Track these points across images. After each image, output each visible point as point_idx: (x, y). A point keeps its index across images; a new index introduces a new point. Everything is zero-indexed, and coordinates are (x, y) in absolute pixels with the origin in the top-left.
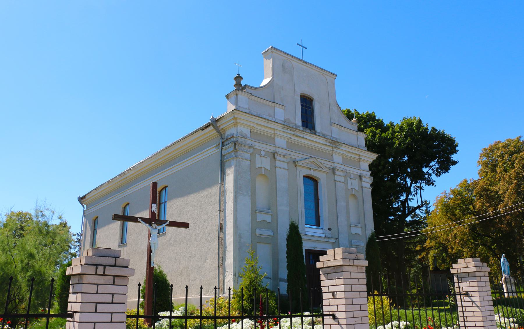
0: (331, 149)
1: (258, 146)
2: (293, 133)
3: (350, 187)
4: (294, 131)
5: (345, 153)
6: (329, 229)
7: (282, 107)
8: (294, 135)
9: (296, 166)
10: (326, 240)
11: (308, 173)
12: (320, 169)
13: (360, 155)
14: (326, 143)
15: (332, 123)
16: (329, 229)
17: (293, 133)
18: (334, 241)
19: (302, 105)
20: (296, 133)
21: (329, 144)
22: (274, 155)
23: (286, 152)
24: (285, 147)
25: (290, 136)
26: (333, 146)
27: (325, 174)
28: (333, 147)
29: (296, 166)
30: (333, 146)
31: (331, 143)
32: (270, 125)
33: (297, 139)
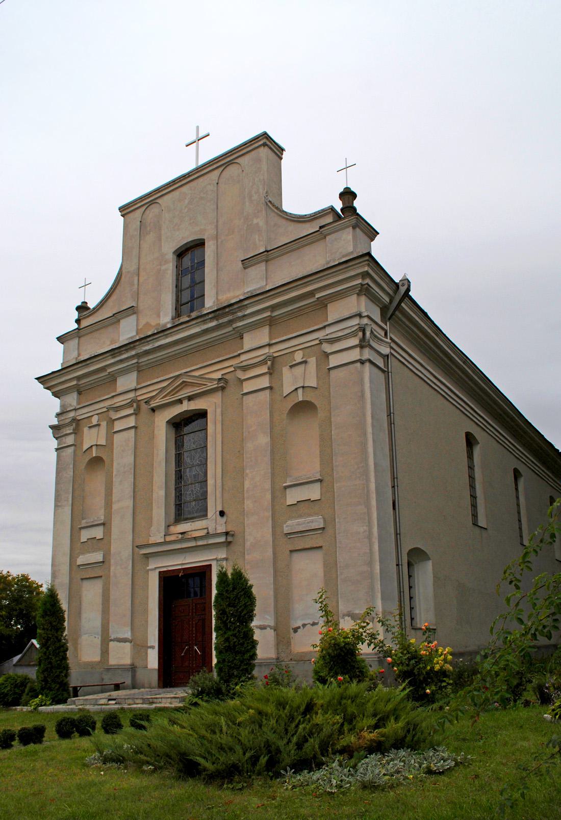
0: (231, 329)
1: (82, 414)
2: (133, 353)
3: (287, 390)
4: (133, 348)
6: (222, 514)
7: (130, 311)
9: (153, 410)
10: (211, 541)
13: (311, 294)
15: (247, 263)
16: (222, 514)
17: (133, 353)
18: (222, 539)
21: (214, 323)
25: (135, 361)
26: (225, 320)
30: (225, 320)
31: (216, 318)
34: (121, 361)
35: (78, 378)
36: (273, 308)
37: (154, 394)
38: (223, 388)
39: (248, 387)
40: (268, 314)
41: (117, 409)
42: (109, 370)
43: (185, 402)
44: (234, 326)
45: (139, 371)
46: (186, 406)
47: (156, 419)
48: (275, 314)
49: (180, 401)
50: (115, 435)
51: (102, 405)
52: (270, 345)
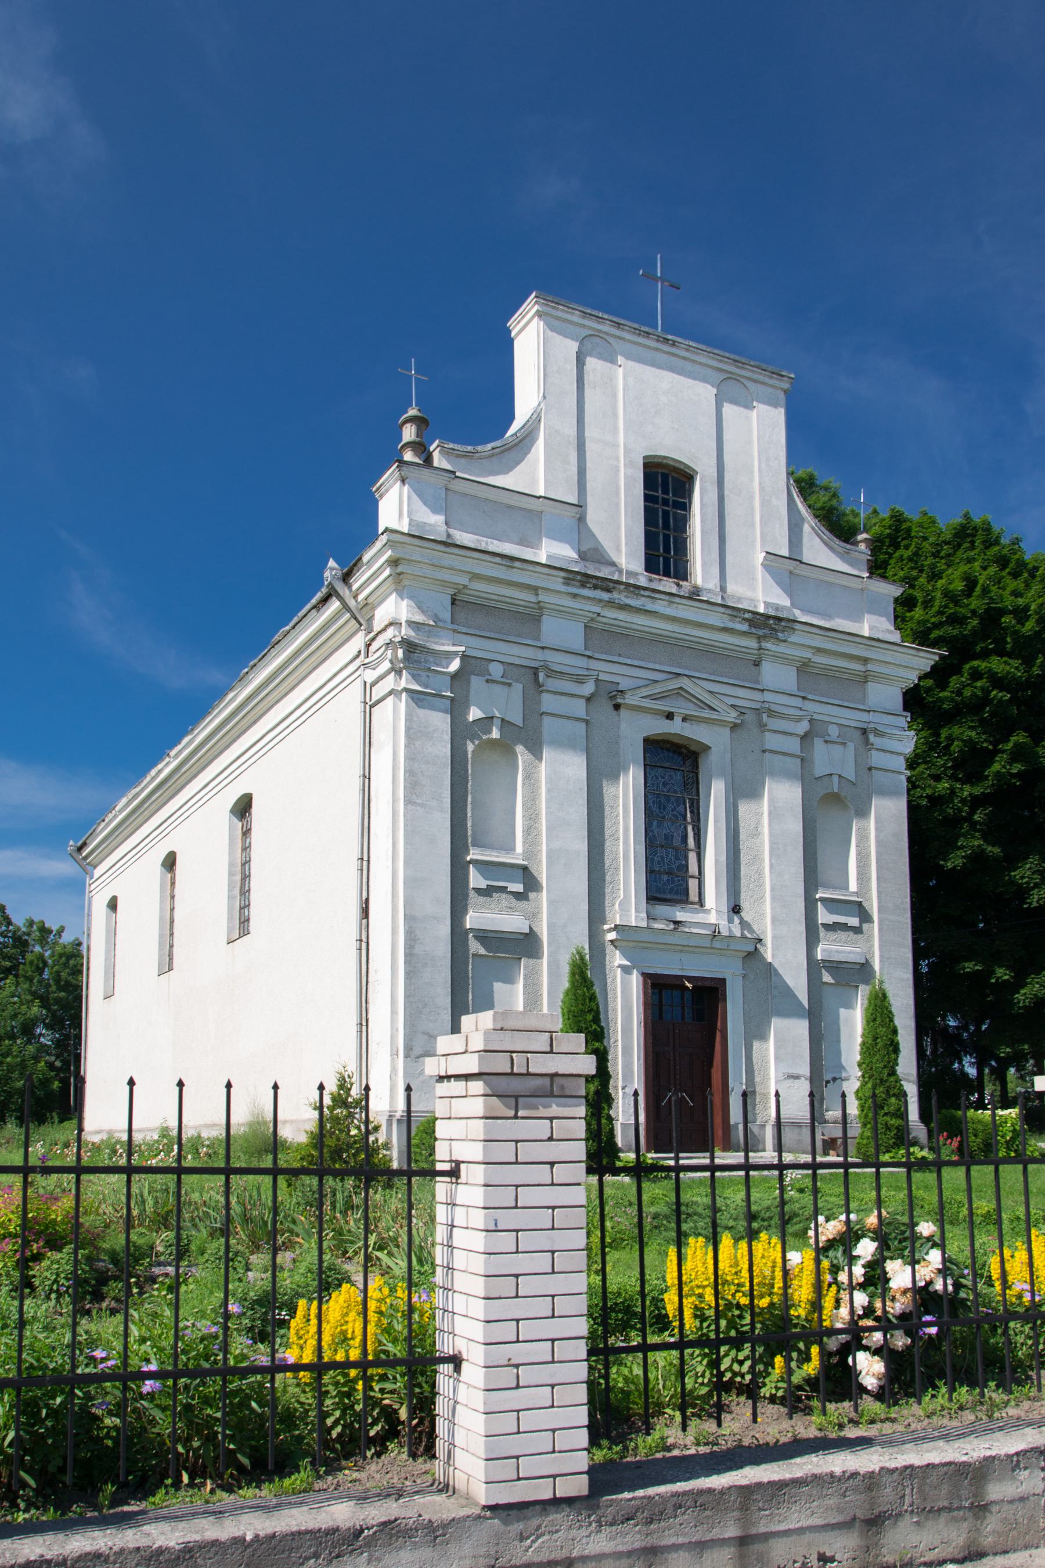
0: (752, 643)
2: (605, 596)
4: (608, 590)
5: (808, 654)
8: (610, 604)
9: (617, 707)
11: (661, 727)
12: (707, 714)
13: (865, 660)
14: (730, 625)
19: (647, 498)
20: (615, 595)
21: (744, 627)
22: (534, 677)
23: (582, 662)
24: (578, 644)
25: (598, 609)
26: (760, 633)
27: (727, 731)
28: (759, 638)
29: (617, 707)
30: (760, 633)
31: (751, 623)
32: (516, 576)
33: (622, 615)
34: (575, 596)
35: (475, 577)
36: (819, 650)
37: (624, 684)
38: (735, 727)
39: (772, 741)
40: (809, 655)
41: (551, 673)
42: (541, 598)
43: (678, 719)
44: (764, 645)
45: (586, 626)
46: (676, 728)
47: (623, 726)
48: (815, 659)
49: (670, 716)
50: (545, 718)
51: (516, 650)
52: (804, 698)
